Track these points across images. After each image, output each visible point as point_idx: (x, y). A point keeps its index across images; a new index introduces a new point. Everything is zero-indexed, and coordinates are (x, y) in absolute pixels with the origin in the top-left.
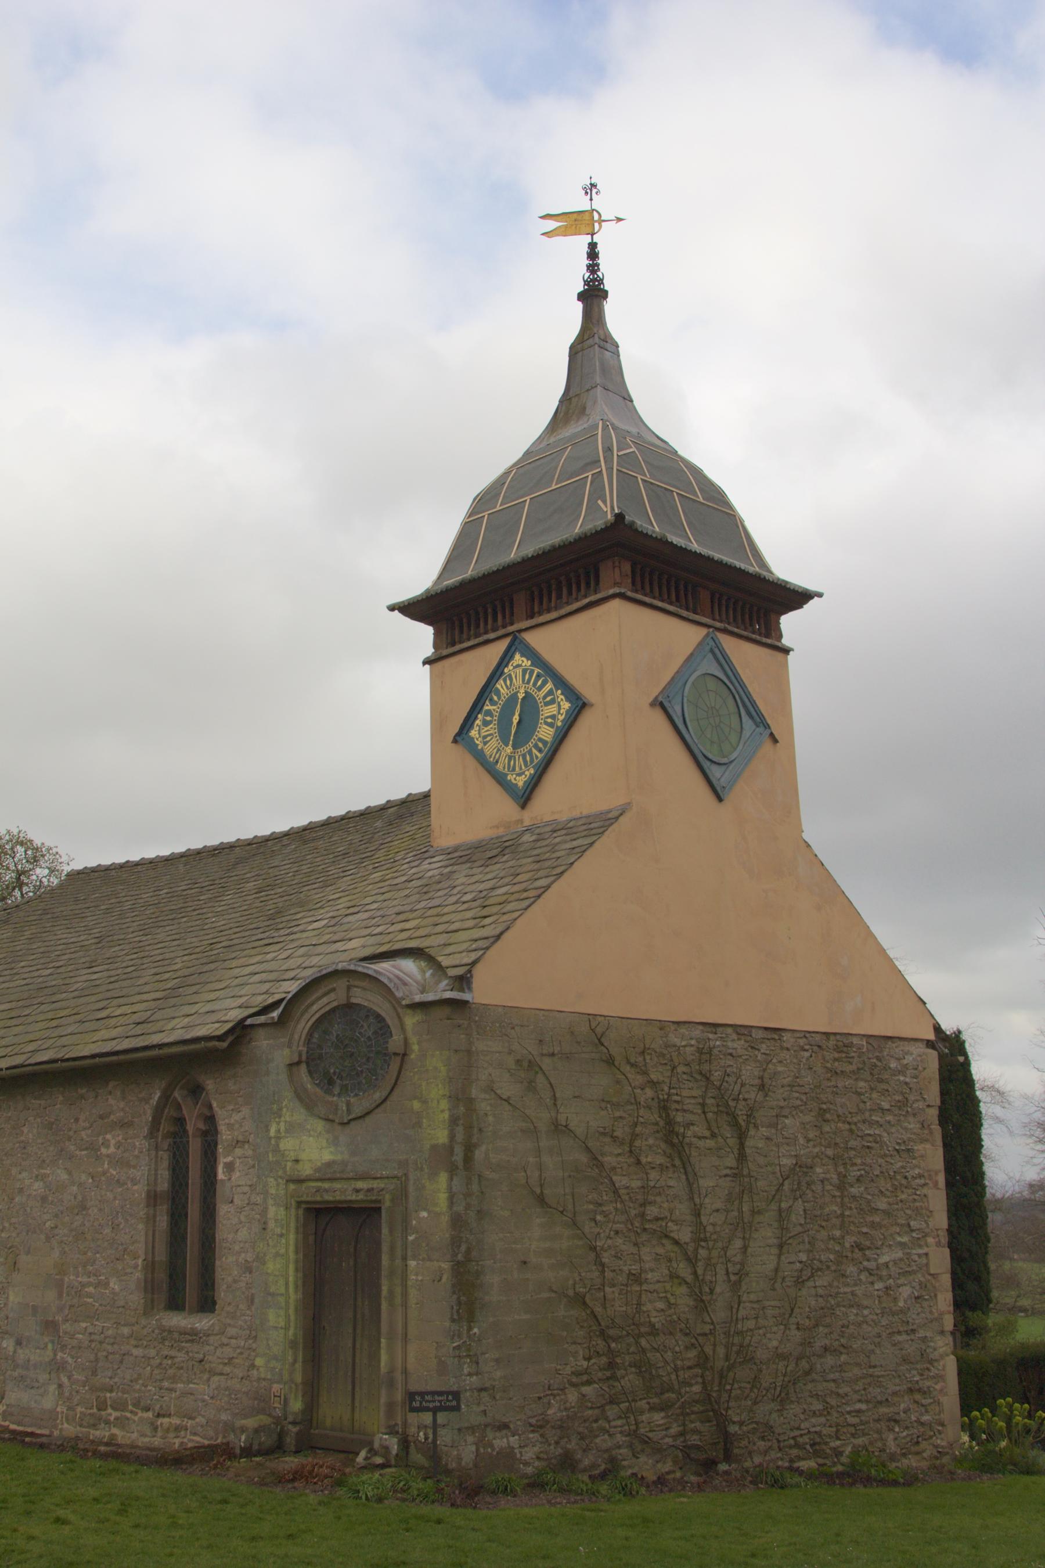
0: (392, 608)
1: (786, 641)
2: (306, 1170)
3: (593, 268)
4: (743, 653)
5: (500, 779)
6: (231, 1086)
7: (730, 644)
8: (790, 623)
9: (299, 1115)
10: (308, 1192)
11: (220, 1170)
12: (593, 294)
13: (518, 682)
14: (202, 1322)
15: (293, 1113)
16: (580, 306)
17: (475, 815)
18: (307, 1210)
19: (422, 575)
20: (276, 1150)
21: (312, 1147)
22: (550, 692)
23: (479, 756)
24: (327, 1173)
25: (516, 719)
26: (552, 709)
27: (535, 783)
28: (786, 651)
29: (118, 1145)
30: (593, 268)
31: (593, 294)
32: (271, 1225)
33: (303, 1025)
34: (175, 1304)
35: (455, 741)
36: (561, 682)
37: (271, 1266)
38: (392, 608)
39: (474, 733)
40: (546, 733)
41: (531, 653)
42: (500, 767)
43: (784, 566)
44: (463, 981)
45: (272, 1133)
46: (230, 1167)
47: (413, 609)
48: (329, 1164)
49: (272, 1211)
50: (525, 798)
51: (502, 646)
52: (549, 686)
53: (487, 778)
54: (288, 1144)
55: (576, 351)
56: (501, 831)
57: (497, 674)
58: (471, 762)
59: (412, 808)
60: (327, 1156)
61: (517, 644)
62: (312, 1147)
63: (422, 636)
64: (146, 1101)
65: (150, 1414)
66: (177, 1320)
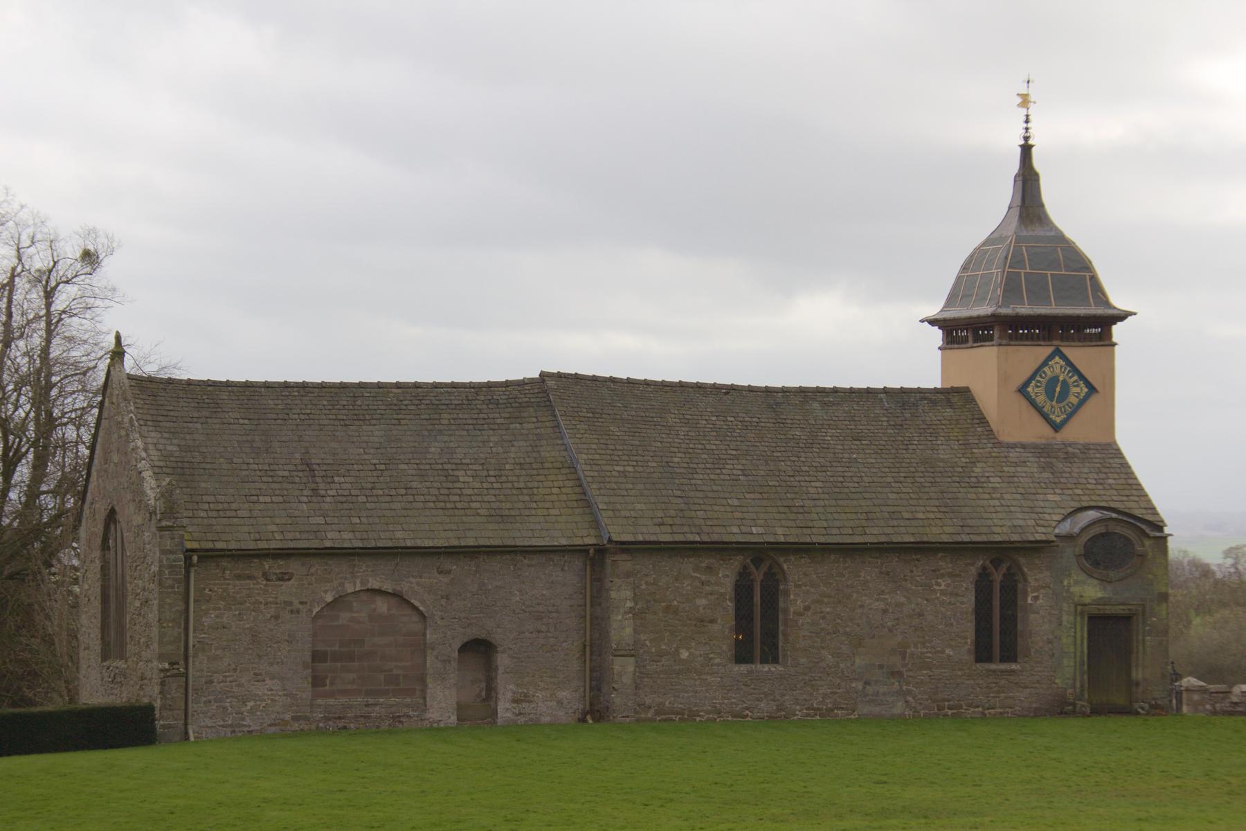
2: (1087, 601)
5: (1045, 417)
6: (1037, 561)
9: (1083, 577)
10: (1094, 610)
12: (1026, 150)
13: (1057, 371)
14: (1014, 666)
18: (1092, 618)
20: (1068, 591)
21: (1091, 591)
23: (1033, 403)
24: (1099, 602)
25: (1058, 389)
26: (1078, 390)
27: (1064, 422)
29: (948, 585)
31: (1026, 150)
32: (1065, 623)
34: (978, 659)
36: (1082, 377)
37: (1064, 641)
39: (1029, 389)
40: (1073, 400)
42: (1045, 410)
45: (1065, 583)
46: (1036, 598)
48: (1101, 599)
49: (1065, 618)
50: (1056, 428)
51: (1048, 350)
52: (1076, 378)
53: (1033, 411)
54: (1076, 589)
56: (1043, 441)
57: (1045, 363)
60: (1100, 595)
61: (1058, 352)
62: (1091, 591)
64: (972, 565)
66: (993, 666)
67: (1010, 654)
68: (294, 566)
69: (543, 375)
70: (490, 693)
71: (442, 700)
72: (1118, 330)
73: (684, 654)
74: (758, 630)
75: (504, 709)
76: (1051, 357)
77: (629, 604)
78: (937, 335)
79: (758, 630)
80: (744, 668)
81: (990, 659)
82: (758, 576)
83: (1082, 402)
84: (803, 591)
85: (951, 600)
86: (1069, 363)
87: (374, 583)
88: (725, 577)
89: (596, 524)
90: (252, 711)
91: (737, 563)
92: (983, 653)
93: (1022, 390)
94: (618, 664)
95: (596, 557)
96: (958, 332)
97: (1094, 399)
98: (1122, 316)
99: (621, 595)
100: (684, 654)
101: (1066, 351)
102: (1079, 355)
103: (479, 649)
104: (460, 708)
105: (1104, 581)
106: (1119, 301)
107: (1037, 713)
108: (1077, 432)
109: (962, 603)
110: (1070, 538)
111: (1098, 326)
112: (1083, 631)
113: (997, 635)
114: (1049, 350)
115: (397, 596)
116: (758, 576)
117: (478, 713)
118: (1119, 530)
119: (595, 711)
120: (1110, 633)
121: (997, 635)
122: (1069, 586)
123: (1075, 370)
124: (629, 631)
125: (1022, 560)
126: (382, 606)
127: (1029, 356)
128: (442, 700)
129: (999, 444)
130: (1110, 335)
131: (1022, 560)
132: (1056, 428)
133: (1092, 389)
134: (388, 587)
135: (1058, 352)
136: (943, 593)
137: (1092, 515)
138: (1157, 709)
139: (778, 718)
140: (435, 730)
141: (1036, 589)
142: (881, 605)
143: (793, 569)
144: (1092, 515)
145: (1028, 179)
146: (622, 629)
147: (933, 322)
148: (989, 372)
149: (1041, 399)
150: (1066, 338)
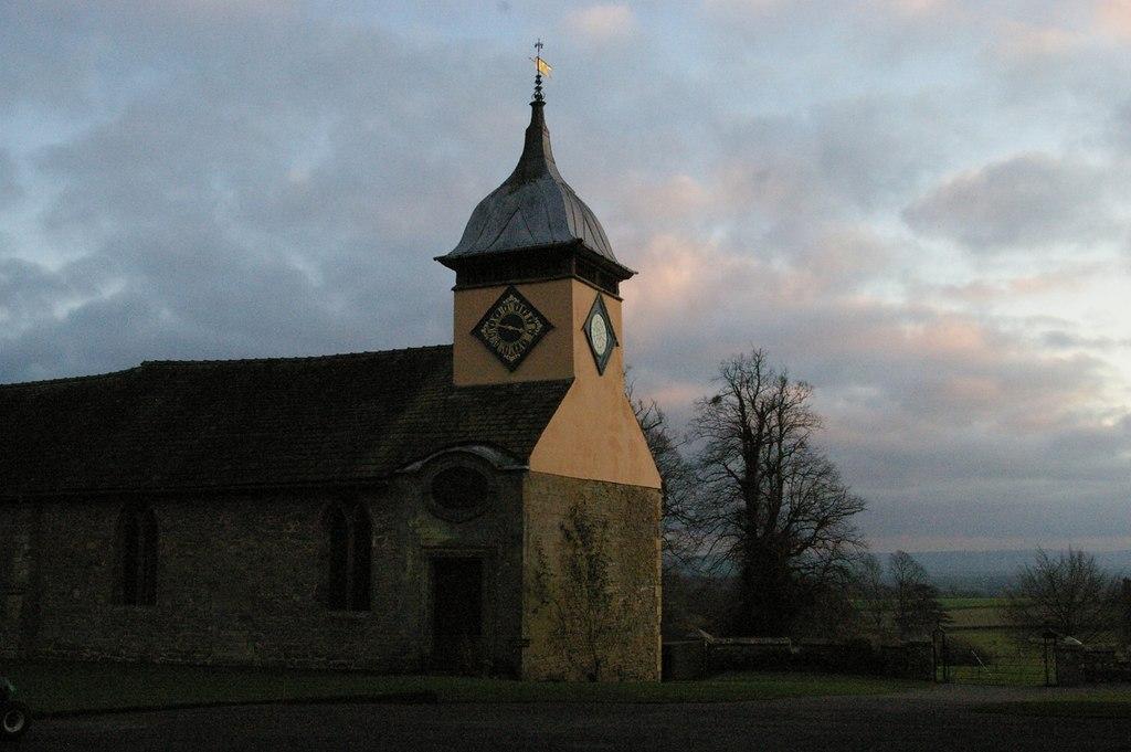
0: (435, 259)
1: (620, 296)
3: (538, 89)
4: (608, 300)
5: (500, 356)
7: (605, 297)
8: (623, 286)
11: (374, 542)
12: (538, 105)
14: (362, 615)
16: (531, 108)
17: (477, 370)
19: (449, 245)
20: (413, 533)
21: (436, 533)
22: (531, 318)
23: (487, 345)
24: (445, 545)
26: (533, 326)
27: (519, 362)
28: (621, 300)
30: (538, 89)
31: (538, 105)
35: (472, 333)
36: (537, 313)
38: (435, 259)
40: (528, 337)
41: (518, 295)
43: (622, 259)
44: (525, 461)
46: (379, 542)
47: (444, 260)
49: (409, 563)
50: (513, 367)
55: (529, 132)
57: (498, 303)
58: (481, 349)
59: (433, 360)
60: (447, 537)
61: (511, 291)
62: (436, 533)
63: (450, 276)
65: (324, 659)
76: (505, 296)
77: (26, 547)
83: (538, 339)
86: (523, 300)
93: (476, 332)
97: (551, 337)
100: (77, 593)
101: (520, 289)
109: (309, 546)
114: (501, 291)
118: (467, 464)
122: (415, 527)
123: (530, 308)
133: (548, 327)
136: (292, 536)
141: (381, 532)
145: (536, 134)
149: (494, 340)
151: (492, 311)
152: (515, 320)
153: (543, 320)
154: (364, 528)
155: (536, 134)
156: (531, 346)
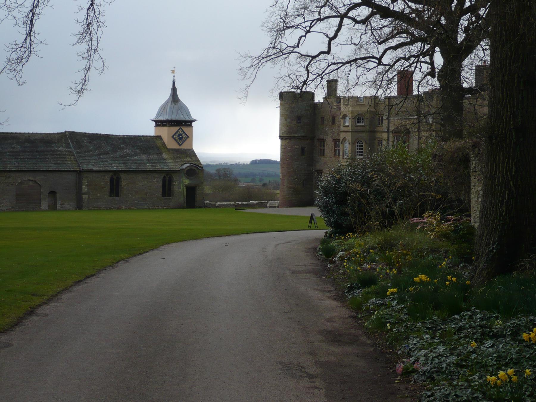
5: (178, 143)
12: (174, 83)
15: (184, 178)
21: (187, 182)
23: (175, 140)
31: (174, 83)
33: (186, 170)
50: (180, 145)
51: (178, 128)
54: (184, 181)
57: (178, 131)
61: (181, 128)
62: (187, 182)
67: (169, 195)
68: (12, 174)
69: (65, 131)
70: (55, 204)
71: (45, 205)
72: (193, 124)
73: (99, 195)
74: (115, 188)
75: (58, 206)
78: (154, 123)
79: (115, 188)
80: (111, 198)
81: (165, 196)
82: (115, 178)
83: (186, 140)
84: (125, 182)
85: (157, 183)
87: (30, 178)
88: (108, 178)
89: (79, 166)
90: (3, 206)
91: (110, 175)
92: (164, 194)
93: (173, 137)
94: (84, 197)
95: (80, 173)
96: (159, 123)
98: (194, 121)
99: (85, 182)
102: (185, 129)
103: (53, 193)
104: (48, 206)
105: (190, 179)
106: (194, 116)
107: (176, 208)
108: (184, 146)
110: (183, 170)
111: (189, 123)
112: (185, 191)
113: (167, 190)
115: (35, 182)
116: (115, 178)
117: (53, 207)
118: (193, 168)
119: (79, 207)
120: (191, 191)
121: (167, 190)
123: (184, 133)
124: (86, 190)
125: (172, 174)
126: (31, 183)
127: (175, 129)
128: (45, 205)
129: (167, 149)
130: (192, 125)
131: (172, 174)
132: (180, 145)
133: (188, 137)
134: (32, 179)
135: (181, 128)
137: (188, 165)
138: (200, 207)
139: (119, 208)
140: (43, 211)
142: (141, 184)
143: (123, 176)
144: (188, 165)
145: (174, 90)
146: (85, 189)
147: (153, 121)
148: (166, 133)
150: (182, 125)
151: (176, 132)
152: (180, 135)
153: (187, 136)
154: (170, 182)
155: (174, 90)
156: (184, 141)
